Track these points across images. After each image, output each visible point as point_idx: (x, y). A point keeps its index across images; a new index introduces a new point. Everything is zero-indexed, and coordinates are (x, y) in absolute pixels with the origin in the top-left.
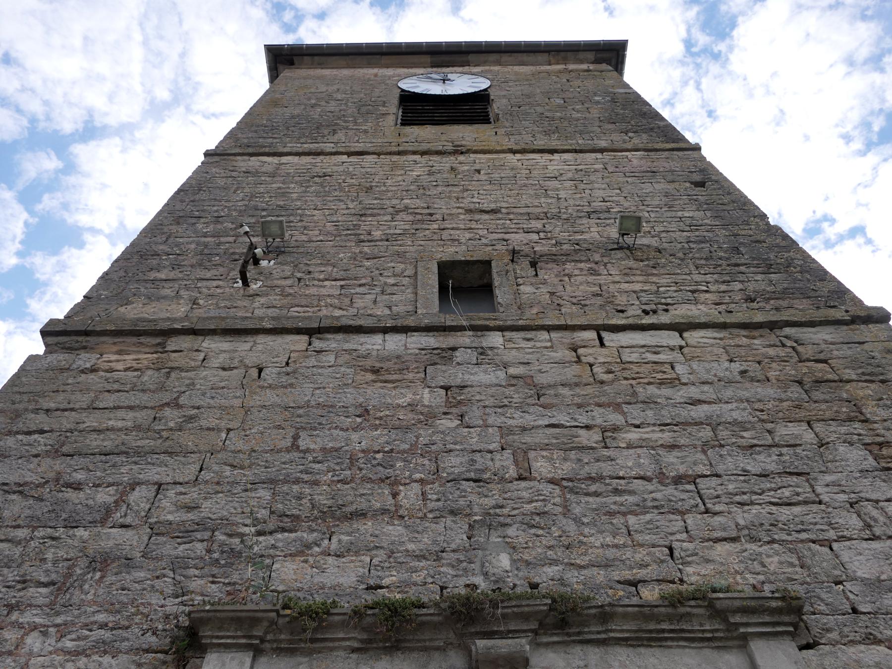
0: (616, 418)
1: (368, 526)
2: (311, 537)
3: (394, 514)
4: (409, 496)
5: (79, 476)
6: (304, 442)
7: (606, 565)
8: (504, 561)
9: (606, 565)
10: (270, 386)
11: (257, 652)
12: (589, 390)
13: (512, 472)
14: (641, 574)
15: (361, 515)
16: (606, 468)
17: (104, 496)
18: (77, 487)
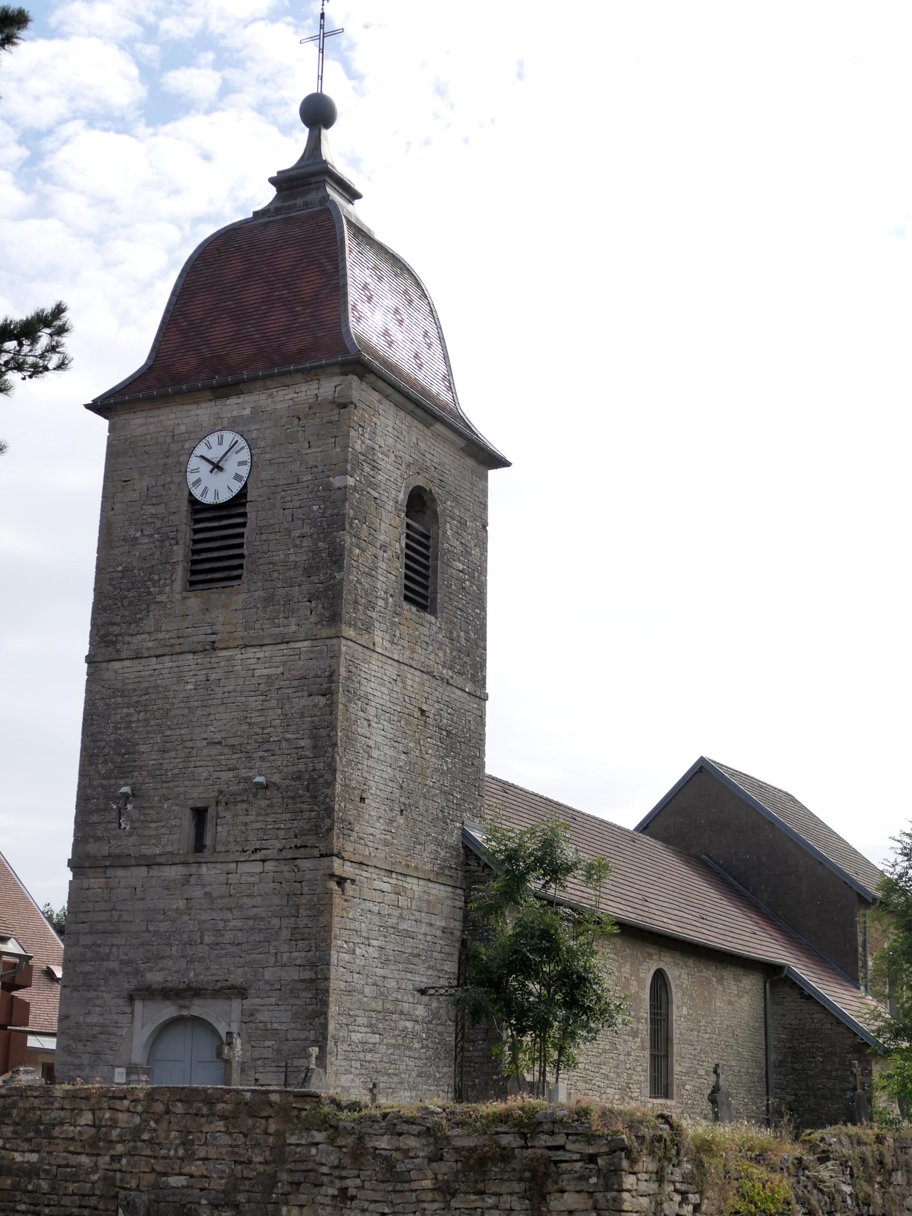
0: (229, 915)
1: (164, 961)
2: (153, 965)
3: (170, 957)
4: (174, 948)
5: (99, 942)
6: (150, 928)
7: (213, 975)
8: (192, 974)
9: (213, 975)
10: (139, 900)
11: (144, 1000)
12: (226, 900)
13: (198, 942)
14: (220, 978)
15: (162, 958)
16: (221, 939)
17: (107, 950)
18: (99, 946)
